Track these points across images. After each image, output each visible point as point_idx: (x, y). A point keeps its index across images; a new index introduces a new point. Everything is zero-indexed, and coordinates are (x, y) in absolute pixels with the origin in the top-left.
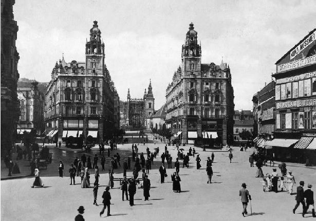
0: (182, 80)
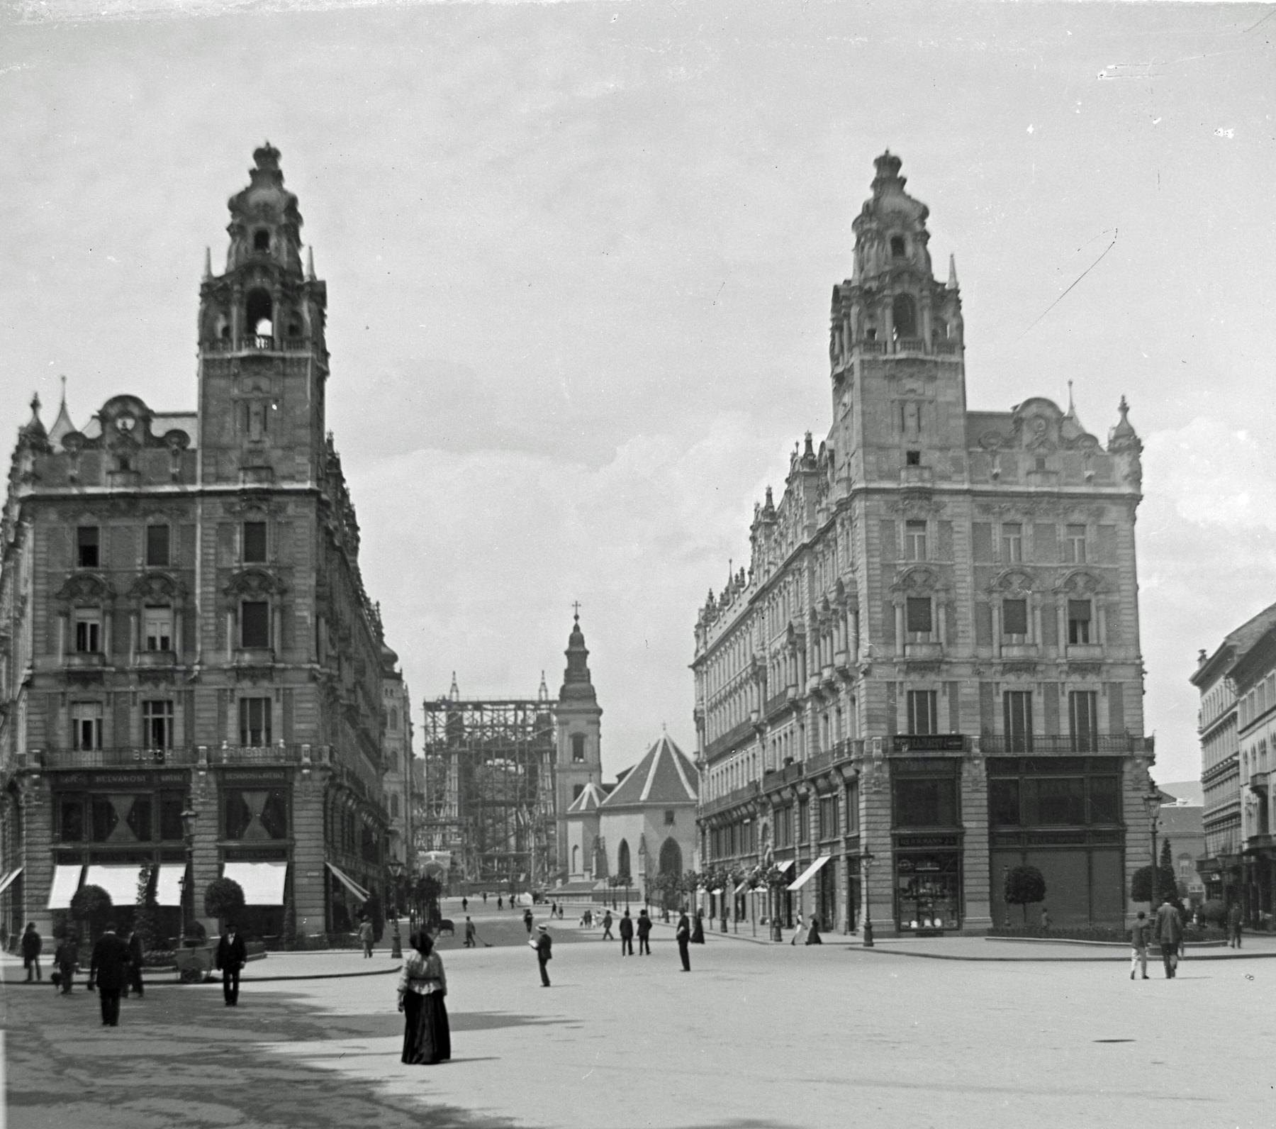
0: (844, 505)
